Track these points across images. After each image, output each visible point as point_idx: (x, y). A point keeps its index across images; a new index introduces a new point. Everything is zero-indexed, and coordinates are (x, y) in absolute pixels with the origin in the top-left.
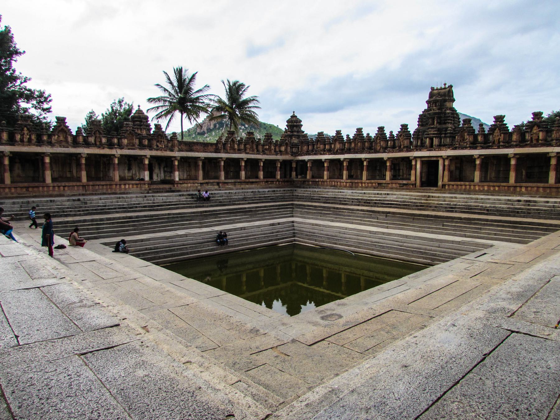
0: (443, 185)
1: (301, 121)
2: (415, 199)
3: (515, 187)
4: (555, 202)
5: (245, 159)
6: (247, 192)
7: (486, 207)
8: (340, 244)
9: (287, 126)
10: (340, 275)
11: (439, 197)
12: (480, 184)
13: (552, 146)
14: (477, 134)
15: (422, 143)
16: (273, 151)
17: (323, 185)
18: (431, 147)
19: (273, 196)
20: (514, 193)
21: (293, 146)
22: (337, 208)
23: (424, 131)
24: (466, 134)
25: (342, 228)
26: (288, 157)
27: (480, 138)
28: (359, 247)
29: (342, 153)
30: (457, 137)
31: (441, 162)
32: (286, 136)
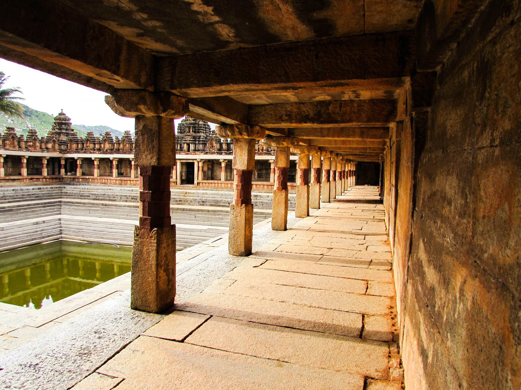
1: (69, 119)
5: (5, 156)
6: (7, 191)
8: (106, 239)
9: (55, 123)
10: (113, 265)
13: (272, 155)
14: (222, 143)
15: (181, 148)
16: (38, 148)
17: (94, 182)
19: (38, 194)
21: (61, 143)
22: (106, 205)
23: (183, 138)
26: (56, 155)
27: (225, 147)
29: (111, 153)
32: (53, 134)
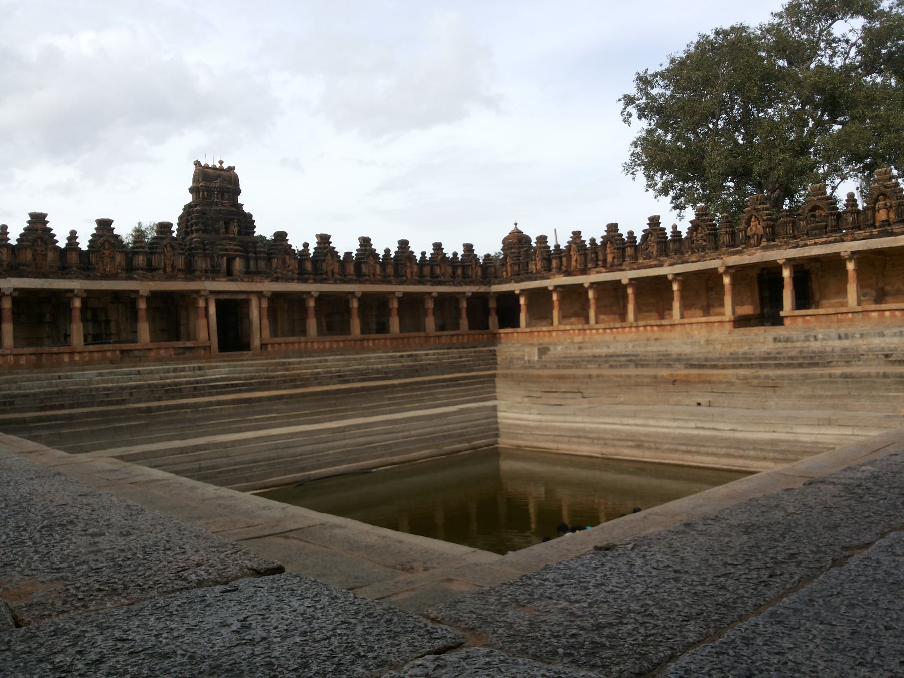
0: (261, 345)
2: (267, 371)
3: (362, 340)
4: (434, 354)
7: (378, 369)
8: (313, 469)
11: (300, 363)
12: (321, 338)
15: (213, 266)
18: (229, 274)
20: (363, 350)
24: (287, 257)
25: (271, 438)
28: (356, 460)
30: (275, 261)
31: (254, 303)
